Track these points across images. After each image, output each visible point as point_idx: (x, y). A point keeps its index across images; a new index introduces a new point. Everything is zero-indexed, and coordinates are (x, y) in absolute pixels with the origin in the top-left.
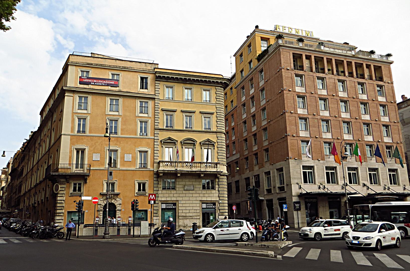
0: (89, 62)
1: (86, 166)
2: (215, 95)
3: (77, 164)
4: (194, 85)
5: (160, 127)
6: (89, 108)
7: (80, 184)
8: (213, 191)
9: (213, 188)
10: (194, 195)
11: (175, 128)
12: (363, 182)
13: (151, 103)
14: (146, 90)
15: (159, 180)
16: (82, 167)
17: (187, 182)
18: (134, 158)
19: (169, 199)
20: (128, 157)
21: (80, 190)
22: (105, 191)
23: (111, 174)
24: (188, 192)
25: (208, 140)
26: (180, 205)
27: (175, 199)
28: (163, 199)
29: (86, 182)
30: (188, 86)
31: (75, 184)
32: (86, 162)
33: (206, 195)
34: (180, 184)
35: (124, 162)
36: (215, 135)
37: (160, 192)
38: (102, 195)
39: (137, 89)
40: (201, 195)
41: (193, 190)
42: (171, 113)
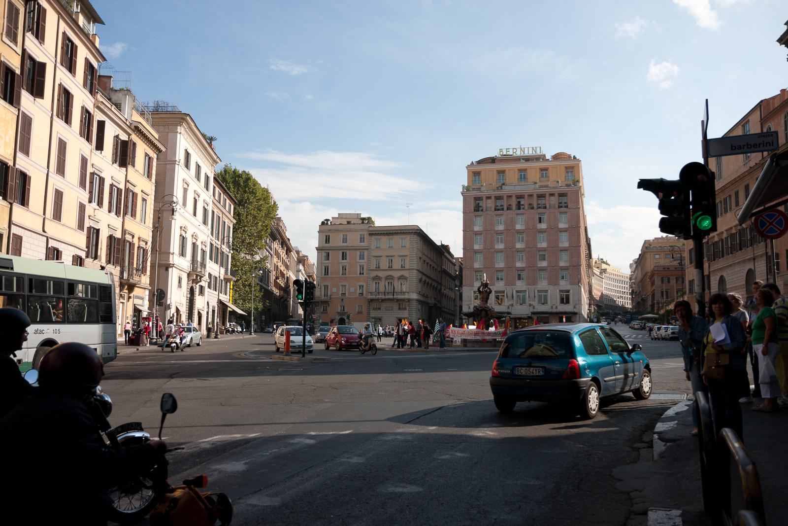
0: (330, 229)
1: (329, 296)
2: (409, 241)
3: (325, 295)
4: (394, 236)
5: (372, 269)
6: (330, 259)
7: (326, 307)
8: (406, 311)
9: (405, 309)
10: (393, 314)
11: (381, 268)
12: (529, 302)
13: (366, 252)
14: (363, 244)
15: (371, 303)
16: (327, 296)
17: (388, 304)
18: (356, 290)
19: (376, 316)
20: (352, 290)
21: (326, 310)
22: (339, 311)
23: (342, 300)
24: (388, 311)
25: (402, 276)
26: (383, 320)
27: (380, 316)
28: (373, 316)
29: (329, 306)
30: (391, 237)
31: (324, 307)
32: (329, 294)
33: (400, 314)
34: (383, 306)
35: (350, 293)
36: (408, 271)
37: (371, 311)
38: (338, 313)
39: (357, 243)
40: (397, 314)
41: (392, 310)
42: (379, 258)
